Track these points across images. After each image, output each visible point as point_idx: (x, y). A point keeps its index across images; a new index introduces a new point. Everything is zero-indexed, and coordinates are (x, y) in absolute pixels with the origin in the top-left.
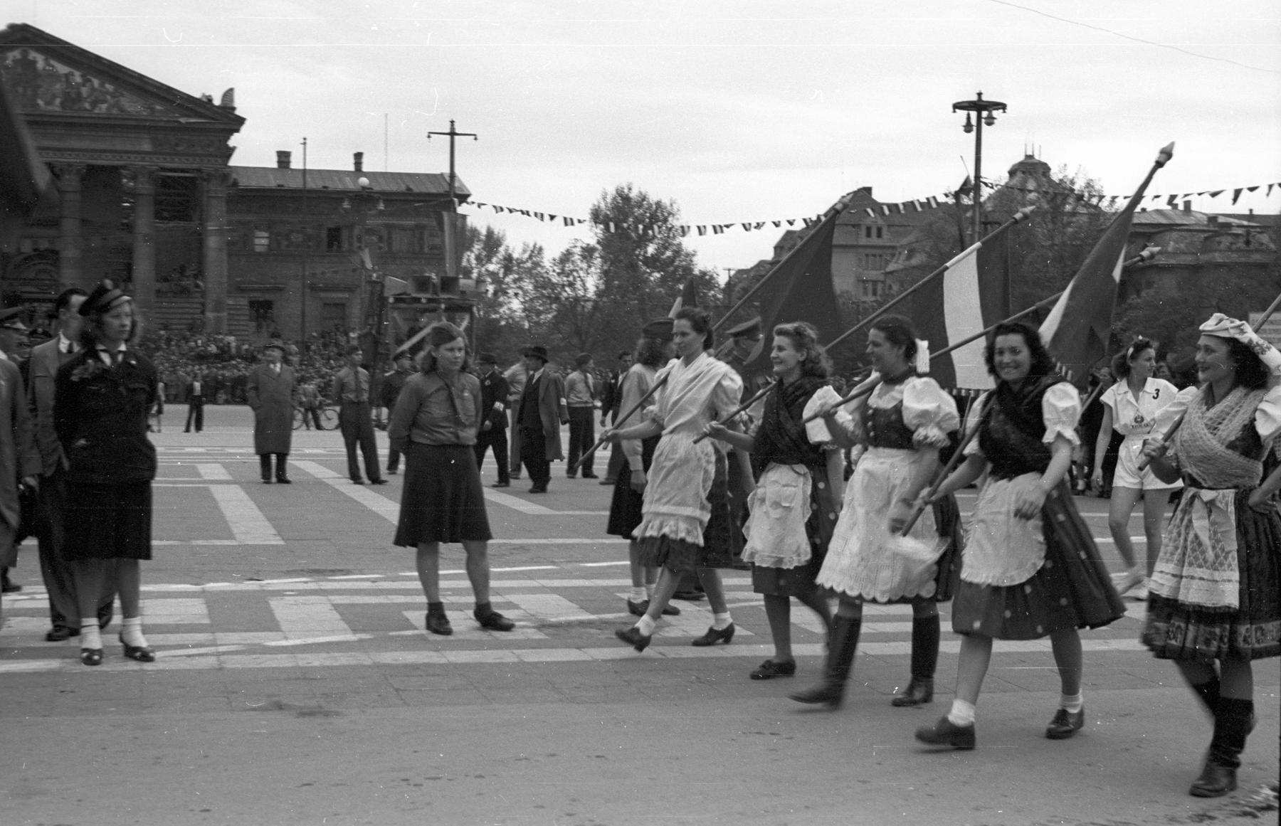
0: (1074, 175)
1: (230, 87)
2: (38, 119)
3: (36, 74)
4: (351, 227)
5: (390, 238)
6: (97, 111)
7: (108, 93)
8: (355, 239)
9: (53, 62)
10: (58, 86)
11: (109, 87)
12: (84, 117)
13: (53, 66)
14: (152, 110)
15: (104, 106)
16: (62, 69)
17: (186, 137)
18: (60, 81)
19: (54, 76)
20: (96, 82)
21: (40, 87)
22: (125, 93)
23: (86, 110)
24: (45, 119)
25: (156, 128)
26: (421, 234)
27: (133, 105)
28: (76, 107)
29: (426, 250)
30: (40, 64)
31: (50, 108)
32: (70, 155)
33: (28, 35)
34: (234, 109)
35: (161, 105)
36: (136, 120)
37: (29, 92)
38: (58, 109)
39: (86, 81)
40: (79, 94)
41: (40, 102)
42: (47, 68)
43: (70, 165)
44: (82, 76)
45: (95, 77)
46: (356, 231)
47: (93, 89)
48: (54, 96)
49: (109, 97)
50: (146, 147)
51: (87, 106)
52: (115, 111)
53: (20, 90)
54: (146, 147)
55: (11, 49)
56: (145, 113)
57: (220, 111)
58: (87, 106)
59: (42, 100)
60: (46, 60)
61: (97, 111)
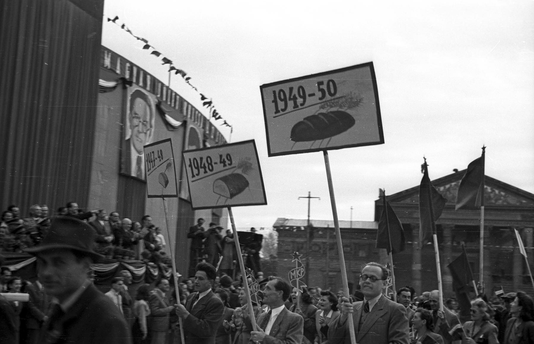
6: (497, 203)
7: (502, 196)
11: (503, 193)
12: (492, 206)
14: (521, 203)
15: (500, 202)
20: (497, 192)
23: (492, 203)
25: (524, 210)
27: (512, 200)
35: (525, 200)
36: (515, 207)
39: (493, 191)
40: (490, 197)
44: (491, 189)
45: (497, 189)
47: (495, 195)
50: (519, 218)
51: (493, 201)
52: (505, 204)
54: (519, 218)
56: (518, 204)
61: (497, 203)
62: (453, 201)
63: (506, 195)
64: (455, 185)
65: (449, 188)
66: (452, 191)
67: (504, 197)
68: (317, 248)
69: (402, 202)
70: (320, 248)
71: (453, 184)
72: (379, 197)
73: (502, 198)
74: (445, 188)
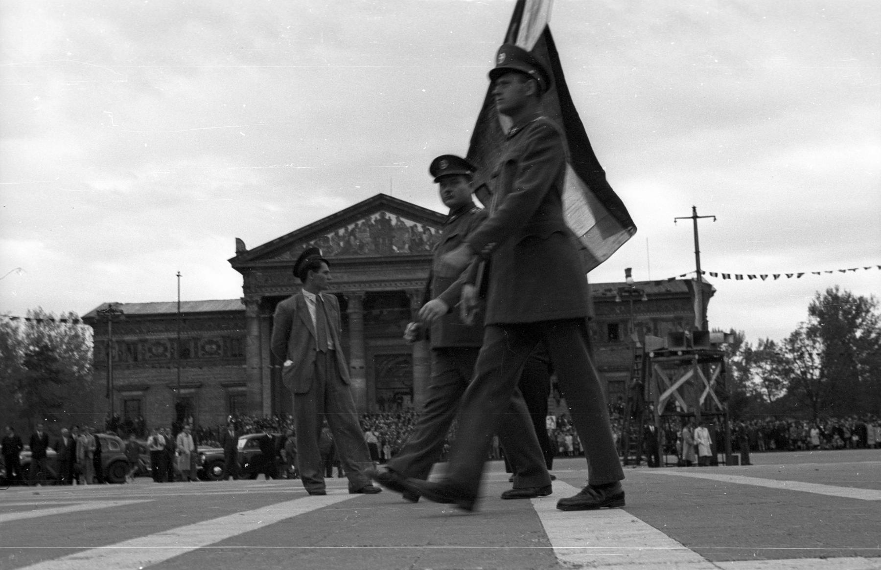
2: (394, 260)
3: (391, 228)
4: (625, 322)
5: (656, 328)
9: (402, 219)
10: (407, 235)
13: (402, 222)
16: (409, 223)
18: (408, 232)
19: (402, 228)
20: (433, 230)
21: (394, 237)
23: (426, 250)
24: (398, 259)
28: (420, 249)
30: (394, 222)
31: (402, 251)
32: (417, 284)
33: (385, 202)
37: (387, 242)
38: (406, 252)
39: (426, 230)
40: (421, 239)
41: (395, 248)
42: (399, 224)
43: (417, 290)
44: (423, 227)
45: (431, 226)
46: (630, 325)
48: (404, 243)
51: (427, 247)
53: (381, 241)
55: (373, 213)
58: (427, 247)
59: (396, 246)
60: (398, 218)
62: (359, 252)
64: (363, 223)
65: (353, 230)
66: (357, 235)
68: (161, 350)
69: (276, 259)
70: (166, 349)
71: (360, 222)
72: (237, 253)
74: (347, 230)
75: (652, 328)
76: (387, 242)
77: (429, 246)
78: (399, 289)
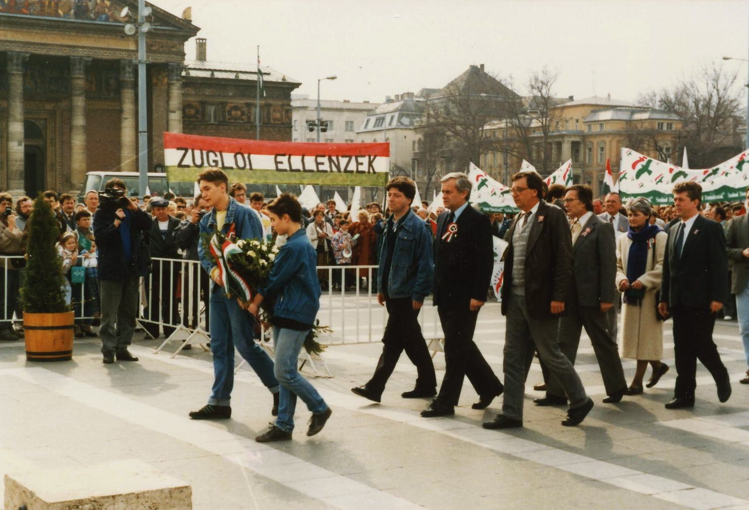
0: (736, 97)
1: (190, 6)
7: (107, 7)
8: (227, 114)
17: (157, 40)
22: (117, 7)
26: (269, 110)
29: (272, 121)
34: (191, 21)
41: (60, 12)
46: (228, 108)
49: (107, 10)
51: (92, 15)
57: (184, 23)
58: (92, 15)
59: (61, 10)
63: (112, 5)
67: (109, 8)
73: (107, 10)
75: (246, 112)
76: (53, 3)
77: (94, 15)
78: (64, 55)
